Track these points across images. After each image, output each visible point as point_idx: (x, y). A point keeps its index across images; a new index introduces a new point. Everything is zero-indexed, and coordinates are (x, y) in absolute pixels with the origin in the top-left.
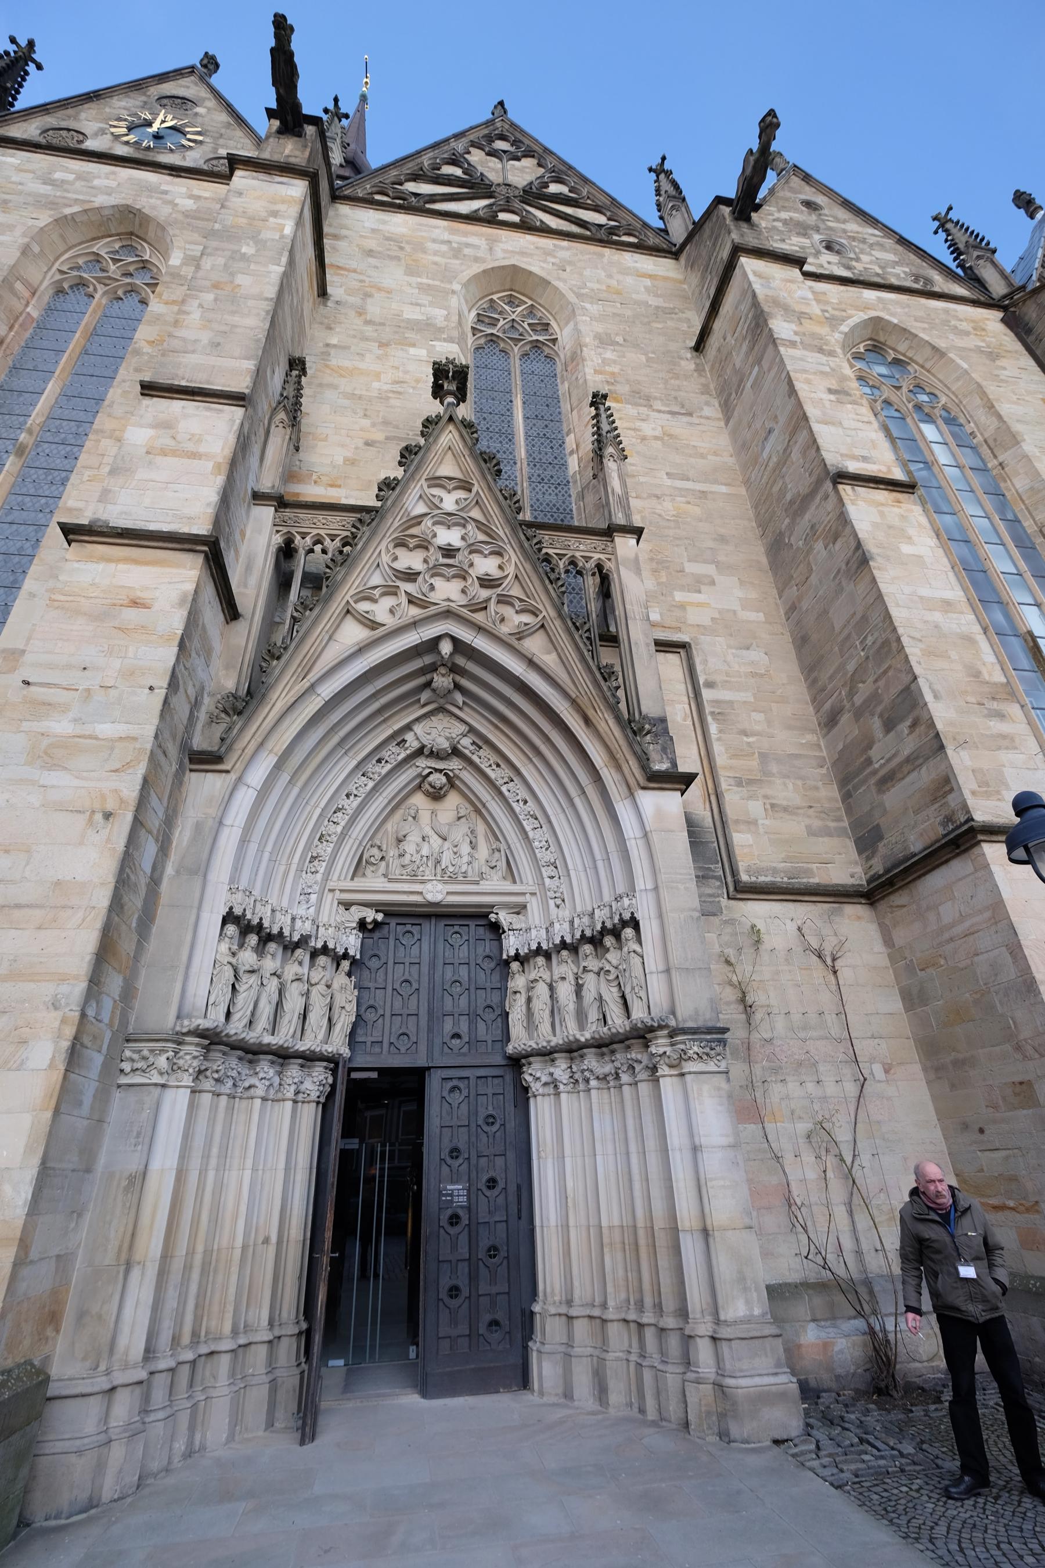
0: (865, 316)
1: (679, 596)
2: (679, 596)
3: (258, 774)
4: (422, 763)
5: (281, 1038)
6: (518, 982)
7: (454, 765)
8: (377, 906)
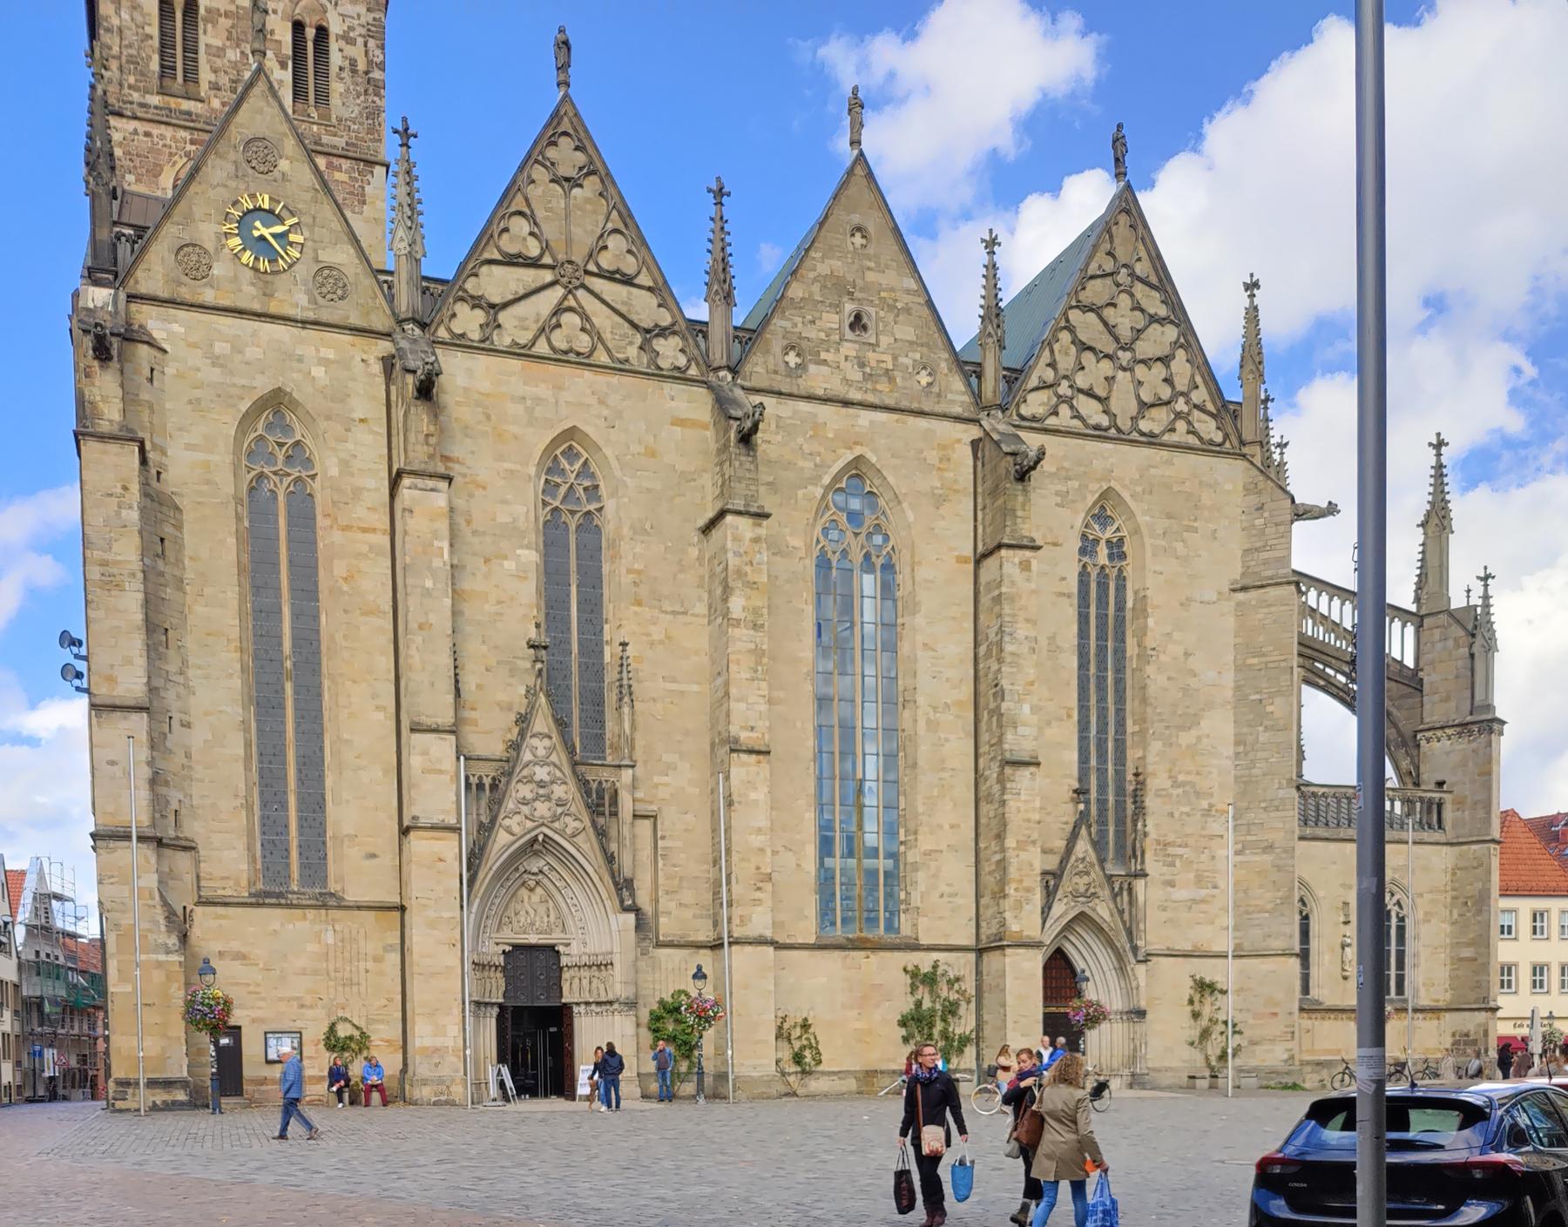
5: (487, 1000)
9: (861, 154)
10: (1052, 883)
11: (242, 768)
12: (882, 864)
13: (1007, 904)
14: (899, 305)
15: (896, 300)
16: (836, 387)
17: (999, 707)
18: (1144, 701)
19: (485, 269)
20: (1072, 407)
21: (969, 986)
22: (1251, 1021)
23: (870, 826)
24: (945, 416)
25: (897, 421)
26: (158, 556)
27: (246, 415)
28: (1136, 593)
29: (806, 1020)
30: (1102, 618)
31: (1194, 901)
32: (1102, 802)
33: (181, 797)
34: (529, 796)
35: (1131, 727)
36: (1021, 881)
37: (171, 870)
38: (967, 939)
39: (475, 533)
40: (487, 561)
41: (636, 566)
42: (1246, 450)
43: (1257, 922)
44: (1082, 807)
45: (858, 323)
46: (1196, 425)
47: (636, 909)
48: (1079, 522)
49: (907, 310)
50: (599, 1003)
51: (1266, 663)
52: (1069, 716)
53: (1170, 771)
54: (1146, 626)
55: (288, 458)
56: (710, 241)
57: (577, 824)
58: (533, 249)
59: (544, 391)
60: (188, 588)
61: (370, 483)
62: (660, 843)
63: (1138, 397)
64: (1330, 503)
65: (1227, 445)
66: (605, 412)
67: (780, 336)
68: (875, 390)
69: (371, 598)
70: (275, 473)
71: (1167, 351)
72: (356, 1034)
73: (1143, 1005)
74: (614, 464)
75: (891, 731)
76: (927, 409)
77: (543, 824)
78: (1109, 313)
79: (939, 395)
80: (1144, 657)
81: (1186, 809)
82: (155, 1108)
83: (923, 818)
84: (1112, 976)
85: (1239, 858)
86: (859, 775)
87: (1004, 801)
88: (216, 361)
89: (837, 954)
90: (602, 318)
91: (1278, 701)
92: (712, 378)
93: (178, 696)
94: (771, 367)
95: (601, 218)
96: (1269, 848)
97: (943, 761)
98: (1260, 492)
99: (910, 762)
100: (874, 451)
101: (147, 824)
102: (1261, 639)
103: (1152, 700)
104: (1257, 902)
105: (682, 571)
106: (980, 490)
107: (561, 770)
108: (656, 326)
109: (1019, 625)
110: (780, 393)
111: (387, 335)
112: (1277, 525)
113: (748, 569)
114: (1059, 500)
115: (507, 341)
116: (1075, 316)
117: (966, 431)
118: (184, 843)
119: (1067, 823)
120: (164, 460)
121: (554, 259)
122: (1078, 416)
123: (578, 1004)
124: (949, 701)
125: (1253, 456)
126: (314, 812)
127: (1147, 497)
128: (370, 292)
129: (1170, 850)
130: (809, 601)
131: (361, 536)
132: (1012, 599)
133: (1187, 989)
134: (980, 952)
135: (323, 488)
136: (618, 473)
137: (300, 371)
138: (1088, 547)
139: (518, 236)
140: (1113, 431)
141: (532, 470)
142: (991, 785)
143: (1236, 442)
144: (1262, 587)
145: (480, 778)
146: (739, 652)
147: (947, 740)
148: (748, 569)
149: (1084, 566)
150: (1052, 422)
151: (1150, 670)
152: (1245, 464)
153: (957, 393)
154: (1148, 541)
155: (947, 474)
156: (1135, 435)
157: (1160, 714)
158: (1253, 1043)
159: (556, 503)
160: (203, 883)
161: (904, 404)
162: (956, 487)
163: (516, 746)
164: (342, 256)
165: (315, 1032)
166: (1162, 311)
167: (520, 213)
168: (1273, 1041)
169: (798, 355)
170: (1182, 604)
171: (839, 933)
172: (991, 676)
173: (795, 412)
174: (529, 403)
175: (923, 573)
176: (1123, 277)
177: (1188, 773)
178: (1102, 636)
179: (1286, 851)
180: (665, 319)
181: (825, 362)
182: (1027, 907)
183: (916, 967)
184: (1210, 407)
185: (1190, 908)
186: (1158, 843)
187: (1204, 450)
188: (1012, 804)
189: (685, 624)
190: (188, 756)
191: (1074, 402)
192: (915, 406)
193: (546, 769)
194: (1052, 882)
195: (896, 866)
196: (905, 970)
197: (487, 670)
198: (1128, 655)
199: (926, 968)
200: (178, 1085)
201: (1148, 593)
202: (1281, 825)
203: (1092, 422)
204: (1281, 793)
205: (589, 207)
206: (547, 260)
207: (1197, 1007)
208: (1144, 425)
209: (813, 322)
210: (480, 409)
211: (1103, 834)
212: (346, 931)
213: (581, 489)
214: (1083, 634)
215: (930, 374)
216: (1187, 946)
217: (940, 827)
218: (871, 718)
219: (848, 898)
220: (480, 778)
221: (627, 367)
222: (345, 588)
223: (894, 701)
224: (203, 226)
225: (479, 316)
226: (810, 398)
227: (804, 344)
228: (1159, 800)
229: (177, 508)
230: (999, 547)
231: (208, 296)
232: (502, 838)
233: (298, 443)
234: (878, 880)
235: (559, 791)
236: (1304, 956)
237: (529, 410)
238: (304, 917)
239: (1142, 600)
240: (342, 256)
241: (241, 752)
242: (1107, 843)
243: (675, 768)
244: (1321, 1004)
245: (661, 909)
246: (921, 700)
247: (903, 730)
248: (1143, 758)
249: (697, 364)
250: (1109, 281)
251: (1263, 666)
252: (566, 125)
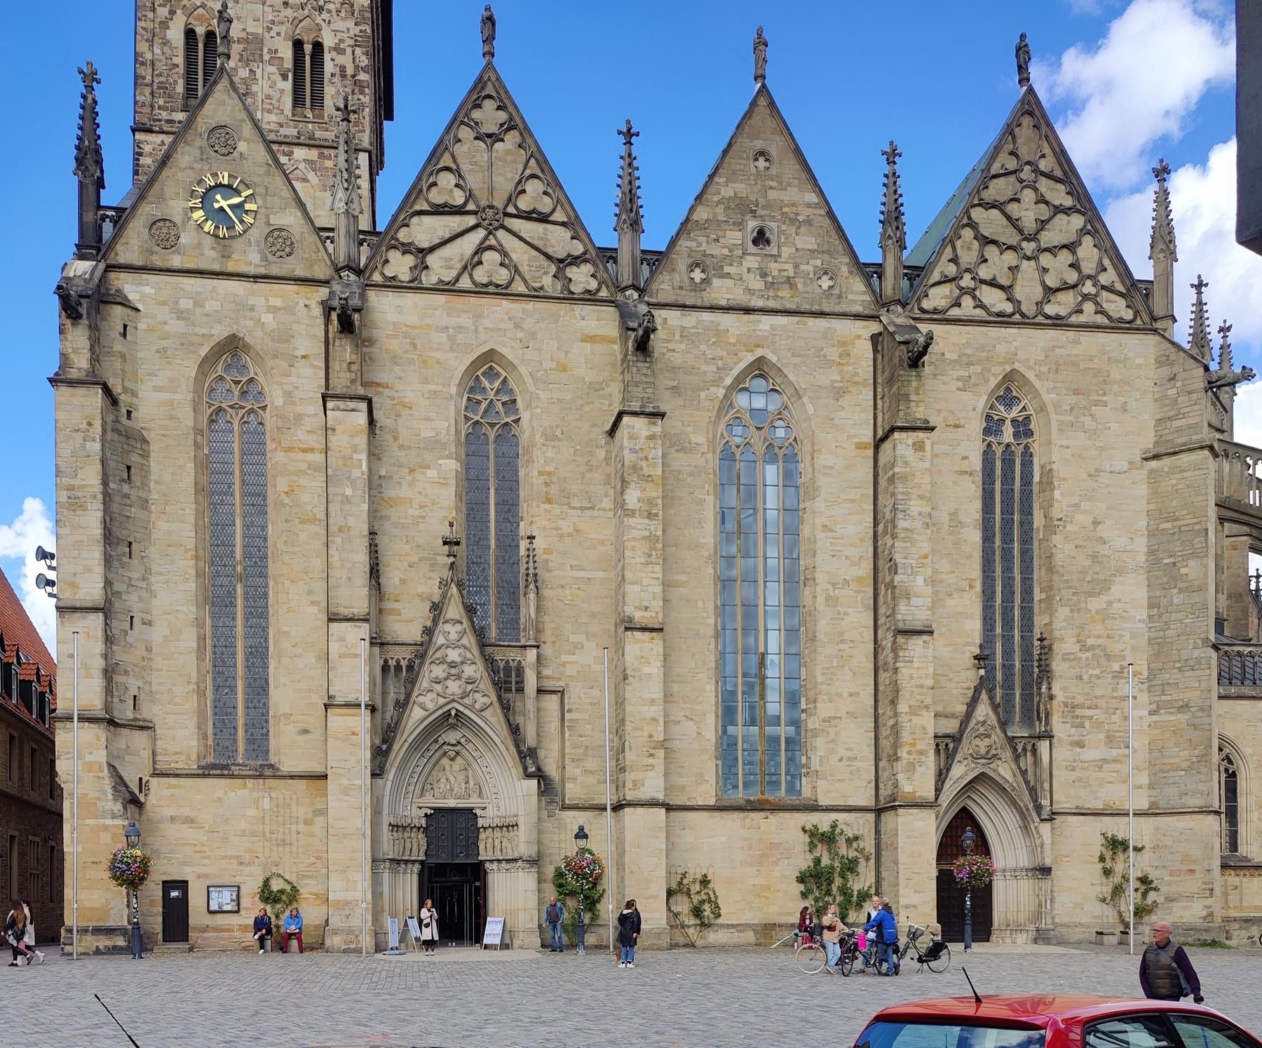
0: (750, 358)
1: (564, 658)
2: (564, 658)
3: (391, 777)
4: (445, 747)
5: (406, 858)
6: (482, 836)
7: (459, 748)
8: (431, 808)
9: (764, 86)
10: (951, 746)
11: (195, 659)
12: (784, 731)
13: (899, 766)
14: (801, 218)
15: (797, 214)
16: (739, 297)
17: (892, 580)
18: (1051, 569)
19: (415, 220)
20: (974, 297)
21: (868, 844)
22: (1167, 878)
23: (772, 696)
24: (844, 315)
25: (798, 323)
26: (123, 481)
27: (205, 360)
28: (1042, 467)
29: (705, 876)
30: (1008, 494)
31: (1105, 761)
32: (1008, 669)
33: (141, 684)
34: (442, 675)
35: (1038, 595)
36: (913, 745)
37: (128, 747)
38: (866, 798)
39: (401, 447)
40: (412, 471)
41: (548, 469)
42: (1158, 325)
43: (1172, 780)
44: (982, 672)
45: (761, 238)
46: (1105, 305)
47: (540, 775)
48: (981, 403)
49: (809, 222)
50: (508, 861)
51: (1180, 527)
52: (971, 587)
53: (1078, 635)
54: (1052, 499)
56: (620, 176)
57: (486, 700)
58: (458, 198)
59: (465, 320)
60: (153, 507)
62: (567, 716)
63: (1043, 283)
64: (1244, 368)
65: (1139, 321)
66: (520, 335)
67: (686, 255)
68: (776, 297)
69: (309, 508)
70: (231, 407)
71: (1073, 238)
72: (288, 888)
73: (1048, 862)
74: (528, 380)
75: (792, 605)
76: (827, 310)
77: (453, 700)
78: (1013, 209)
79: (840, 297)
80: (1050, 528)
81: (1097, 672)
82: (98, 952)
83: (823, 687)
84: (1017, 834)
85: (1154, 718)
86: (762, 649)
87: (897, 668)
88: (181, 315)
89: (736, 815)
90: (519, 252)
91: (1192, 563)
92: (620, 297)
93: (140, 599)
94: (677, 284)
95: (521, 167)
96: (1184, 707)
97: (842, 634)
98: (1172, 364)
99: (810, 636)
100: (775, 352)
101: (100, 707)
102: (1174, 504)
103: (1060, 569)
104: (1174, 761)
105: (590, 470)
106: (879, 380)
107: (470, 651)
108: (569, 255)
109: (912, 503)
110: (684, 306)
111: (326, 282)
112: (1189, 393)
113: (643, 463)
114: (960, 384)
115: (434, 279)
116: (977, 214)
117: (866, 327)
118: (141, 724)
119: (970, 689)
120: (135, 401)
121: (478, 206)
122: (980, 305)
123: (491, 861)
124: (848, 578)
125: (1165, 330)
126: (259, 694)
127: (1052, 376)
128: (314, 248)
129: (1078, 712)
130: (711, 491)
131: (301, 455)
132: (905, 478)
133: (1097, 846)
134: (879, 811)
135: (271, 417)
136: (531, 388)
137: (251, 319)
138: (992, 427)
139: (446, 189)
140: (1017, 316)
141: (453, 390)
142: (886, 655)
143: (1147, 318)
144: (1175, 453)
145: (398, 661)
146: (634, 539)
147: (847, 614)
148: (643, 463)
149: (989, 445)
150: (955, 312)
151: (1056, 539)
152: (1157, 338)
153: (858, 293)
154: (1054, 417)
155: (846, 368)
156: (1040, 319)
157: (1067, 581)
158: (1169, 899)
159: (478, 418)
160: (158, 758)
161: (806, 307)
162: (857, 379)
163: (429, 632)
164: (290, 219)
165: (251, 887)
166: (1068, 202)
167: (447, 169)
168: (1190, 898)
169: (703, 271)
170: (1090, 475)
171: (740, 795)
172: (887, 552)
173: (699, 322)
174: (451, 330)
175: (821, 460)
176: (1027, 174)
177: (1098, 637)
178: (1007, 509)
179: (1202, 710)
180: (577, 248)
181: (728, 275)
182: (920, 770)
183: (815, 827)
184: (1119, 287)
185: (1101, 768)
186: (1066, 705)
187: (1112, 328)
188: (905, 672)
189: (592, 518)
190: (149, 649)
191: (977, 293)
192: (816, 308)
193: (457, 651)
194: (947, 747)
195: (798, 733)
196: (803, 829)
197: (410, 566)
198: (1035, 526)
199: (825, 827)
200: (118, 932)
201: (1054, 467)
202: (1197, 685)
203: (995, 310)
204: (1197, 653)
205: (509, 158)
206: (471, 207)
207: (1108, 864)
208: (1050, 309)
209: (717, 240)
210: (408, 341)
211: (1008, 698)
212: (281, 797)
213: (499, 406)
214: (987, 508)
215: (831, 278)
216: (1097, 805)
217: (839, 695)
218: (773, 595)
219: (751, 763)
220: (398, 661)
221: (541, 293)
222: (287, 501)
223: (794, 580)
224: (172, 203)
225: (410, 260)
226: (713, 308)
227: (708, 261)
228: (1067, 664)
229: (145, 441)
230: (893, 430)
231: (176, 261)
232: (416, 714)
233: (252, 380)
234: (780, 745)
235: (469, 671)
236: (1232, 814)
237: (452, 339)
238: (245, 786)
239: (1048, 473)
240: (290, 219)
241: (194, 645)
242: (1014, 706)
243: (582, 648)
244: (1250, 861)
245: (567, 776)
246: (819, 577)
247: (804, 607)
248: (1050, 624)
249: (607, 287)
250: (1012, 179)
251: (1176, 530)
252: (489, 90)
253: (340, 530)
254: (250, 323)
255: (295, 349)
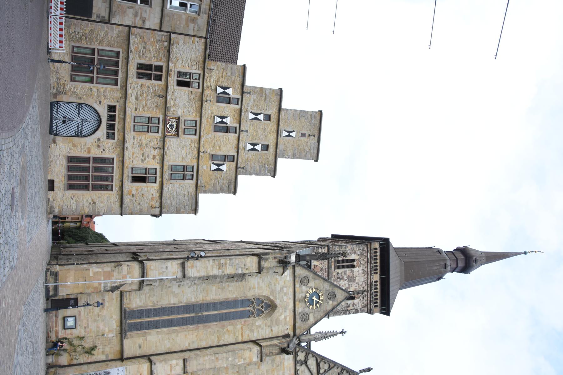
19: (314, 358)
55: (259, 309)
61: (255, 334)
70: (254, 306)
253: (217, 358)
254: (281, 311)
255: (274, 327)
